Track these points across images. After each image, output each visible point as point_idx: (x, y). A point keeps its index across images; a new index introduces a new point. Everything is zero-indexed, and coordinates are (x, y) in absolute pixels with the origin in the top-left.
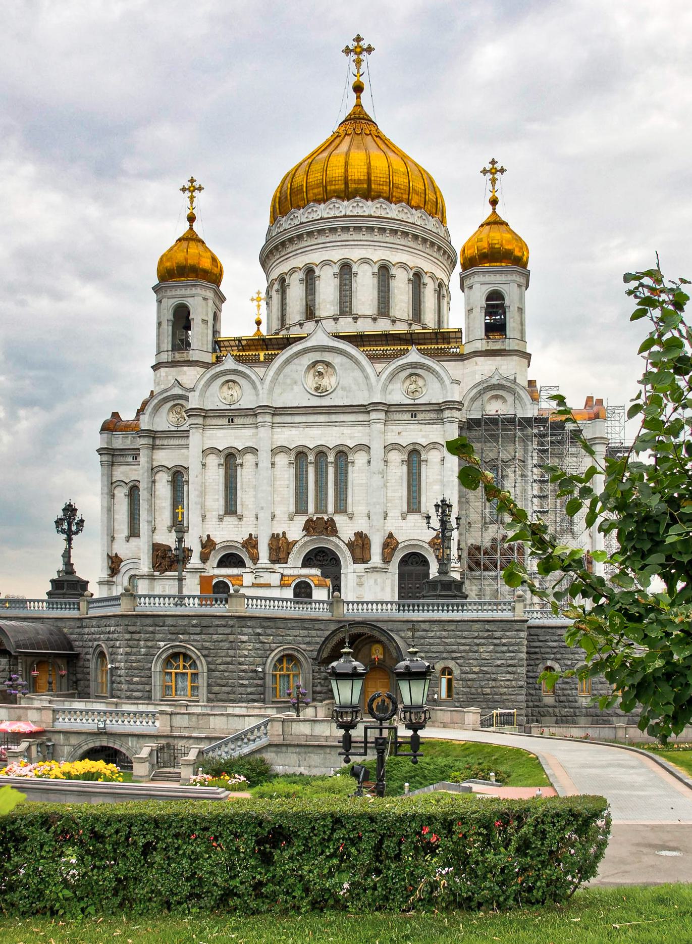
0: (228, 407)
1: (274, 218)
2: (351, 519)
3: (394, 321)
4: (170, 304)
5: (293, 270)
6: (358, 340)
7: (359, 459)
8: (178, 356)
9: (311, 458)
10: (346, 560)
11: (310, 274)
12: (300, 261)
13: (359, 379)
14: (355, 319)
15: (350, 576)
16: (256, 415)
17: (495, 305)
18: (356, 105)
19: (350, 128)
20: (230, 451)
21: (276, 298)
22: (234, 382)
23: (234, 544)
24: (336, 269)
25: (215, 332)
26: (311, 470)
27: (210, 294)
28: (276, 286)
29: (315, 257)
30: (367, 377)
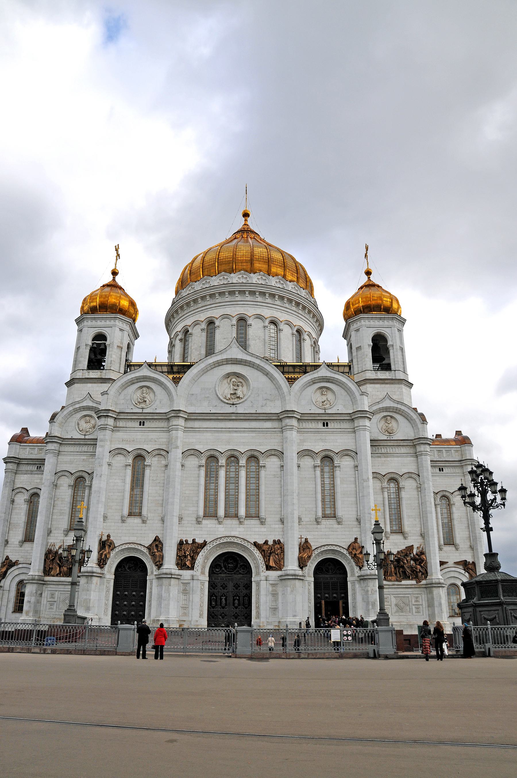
0: (140, 411)
1: (177, 293)
2: (262, 523)
4: (92, 333)
5: (196, 323)
7: (271, 464)
8: (94, 374)
9: (222, 461)
10: (257, 567)
12: (202, 317)
15: (263, 584)
16: (168, 419)
18: (245, 225)
21: (179, 346)
22: (148, 387)
23: (140, 547)
24: (234, 322)
27: (127, 327)
28: (179, 337)
29: (216, 313)
30: (278, 387)
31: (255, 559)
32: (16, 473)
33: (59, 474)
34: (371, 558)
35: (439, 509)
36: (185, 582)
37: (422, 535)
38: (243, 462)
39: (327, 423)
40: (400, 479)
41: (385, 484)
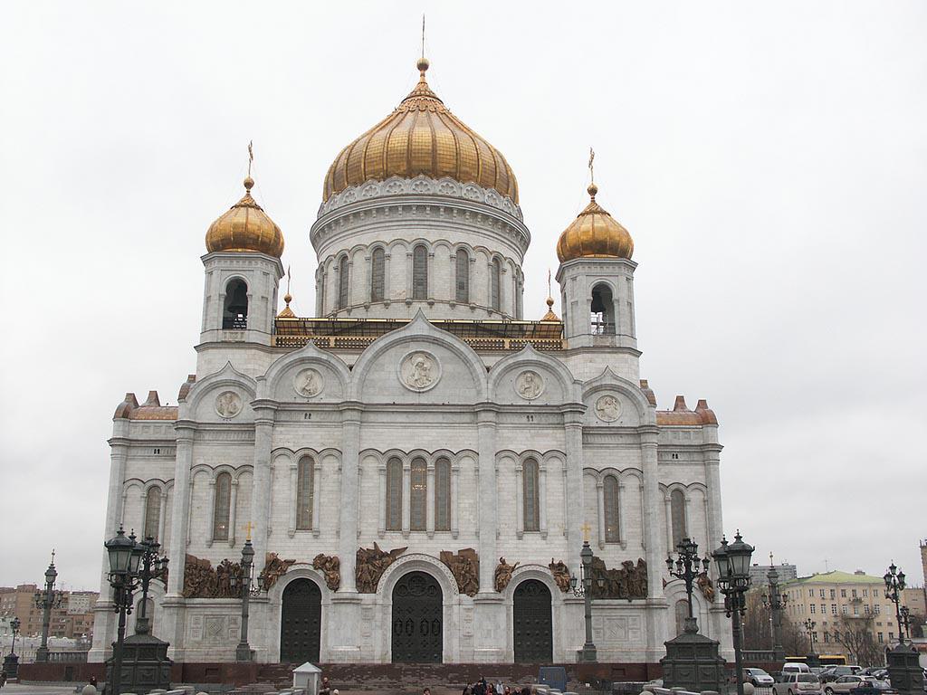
0: (305, 401)
3: (473, 308)
5: (358, 248)
6: (477, 328)
9: (407, 465)
11: (378, 252)
13: (459, 376)
14: (431, 304)
15: (456, 608)
17: (602, 299)
19: (412, 105)
20: (306, 452)
25: (274, 311)
26: (406, 479)
27: (273, 270)
28: (333, 264)
29: (386, 236)
31: (444, 578)
32: (127, 459)
33: (196, 469)
34: (579, 584)
35: (669, 507)
36: (365, 607)
37: (644, 546)
38: (431, 465)
39: (532, 417)
40: (619, 477)
41: (601, 483)
